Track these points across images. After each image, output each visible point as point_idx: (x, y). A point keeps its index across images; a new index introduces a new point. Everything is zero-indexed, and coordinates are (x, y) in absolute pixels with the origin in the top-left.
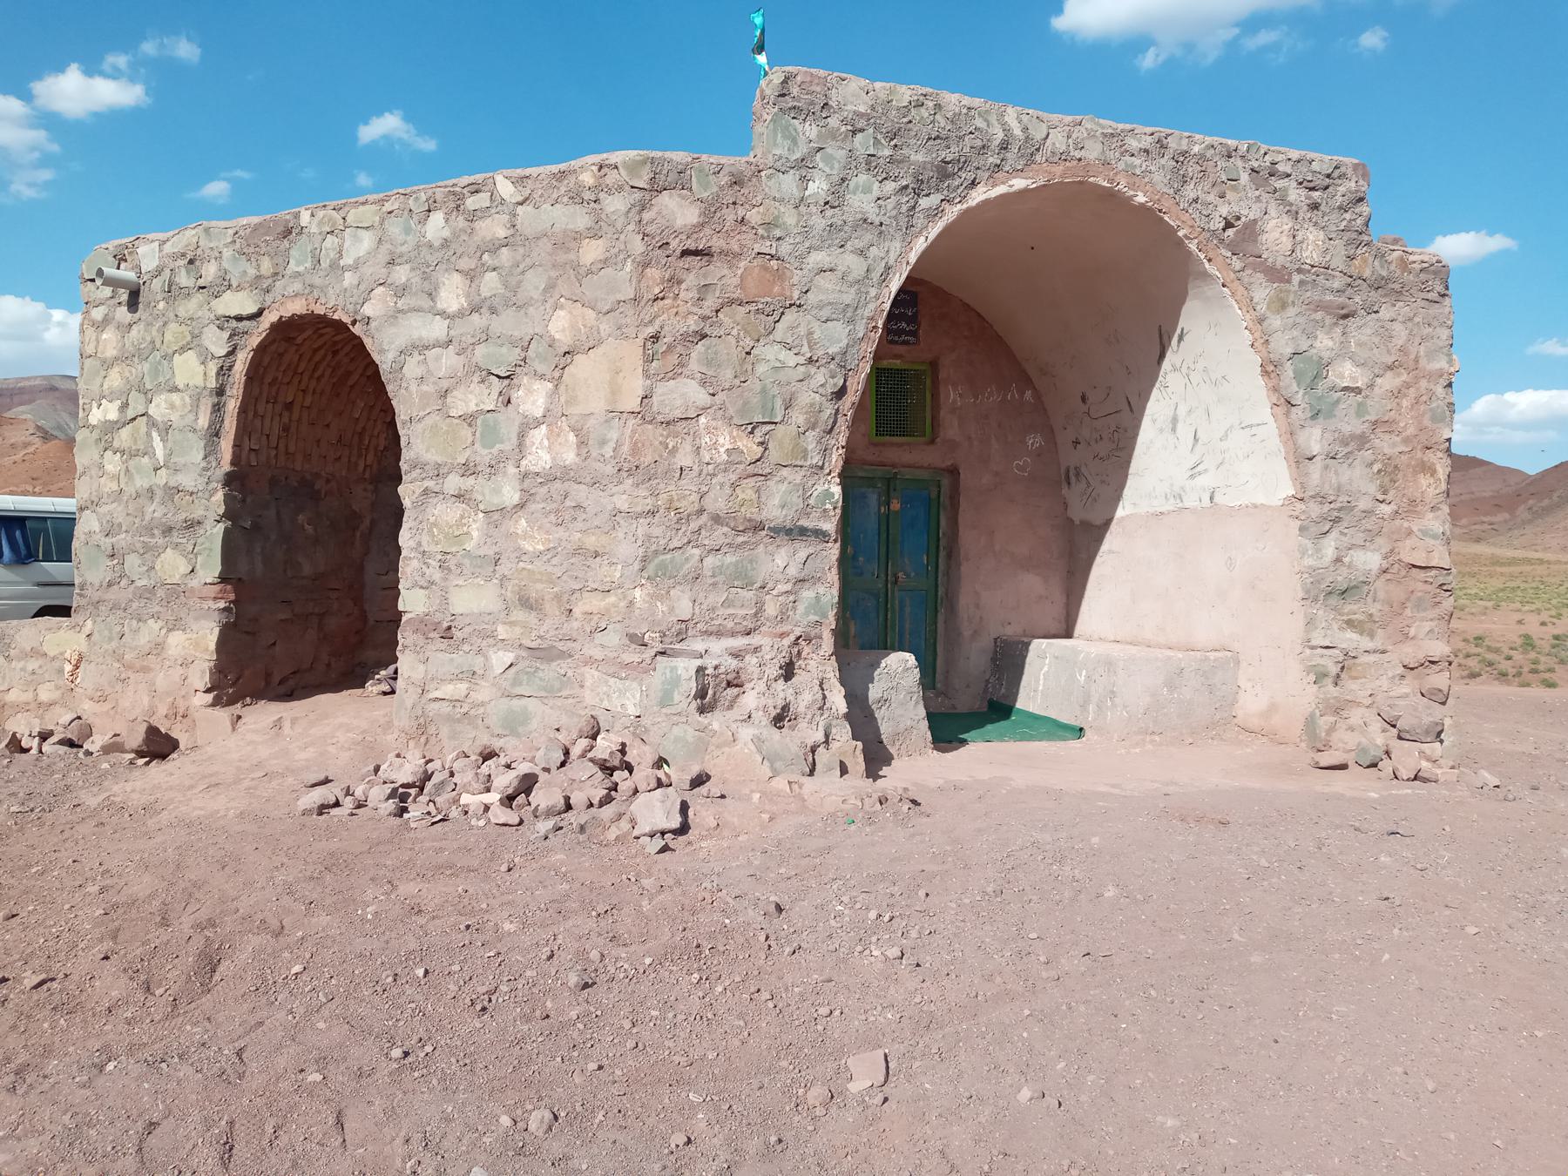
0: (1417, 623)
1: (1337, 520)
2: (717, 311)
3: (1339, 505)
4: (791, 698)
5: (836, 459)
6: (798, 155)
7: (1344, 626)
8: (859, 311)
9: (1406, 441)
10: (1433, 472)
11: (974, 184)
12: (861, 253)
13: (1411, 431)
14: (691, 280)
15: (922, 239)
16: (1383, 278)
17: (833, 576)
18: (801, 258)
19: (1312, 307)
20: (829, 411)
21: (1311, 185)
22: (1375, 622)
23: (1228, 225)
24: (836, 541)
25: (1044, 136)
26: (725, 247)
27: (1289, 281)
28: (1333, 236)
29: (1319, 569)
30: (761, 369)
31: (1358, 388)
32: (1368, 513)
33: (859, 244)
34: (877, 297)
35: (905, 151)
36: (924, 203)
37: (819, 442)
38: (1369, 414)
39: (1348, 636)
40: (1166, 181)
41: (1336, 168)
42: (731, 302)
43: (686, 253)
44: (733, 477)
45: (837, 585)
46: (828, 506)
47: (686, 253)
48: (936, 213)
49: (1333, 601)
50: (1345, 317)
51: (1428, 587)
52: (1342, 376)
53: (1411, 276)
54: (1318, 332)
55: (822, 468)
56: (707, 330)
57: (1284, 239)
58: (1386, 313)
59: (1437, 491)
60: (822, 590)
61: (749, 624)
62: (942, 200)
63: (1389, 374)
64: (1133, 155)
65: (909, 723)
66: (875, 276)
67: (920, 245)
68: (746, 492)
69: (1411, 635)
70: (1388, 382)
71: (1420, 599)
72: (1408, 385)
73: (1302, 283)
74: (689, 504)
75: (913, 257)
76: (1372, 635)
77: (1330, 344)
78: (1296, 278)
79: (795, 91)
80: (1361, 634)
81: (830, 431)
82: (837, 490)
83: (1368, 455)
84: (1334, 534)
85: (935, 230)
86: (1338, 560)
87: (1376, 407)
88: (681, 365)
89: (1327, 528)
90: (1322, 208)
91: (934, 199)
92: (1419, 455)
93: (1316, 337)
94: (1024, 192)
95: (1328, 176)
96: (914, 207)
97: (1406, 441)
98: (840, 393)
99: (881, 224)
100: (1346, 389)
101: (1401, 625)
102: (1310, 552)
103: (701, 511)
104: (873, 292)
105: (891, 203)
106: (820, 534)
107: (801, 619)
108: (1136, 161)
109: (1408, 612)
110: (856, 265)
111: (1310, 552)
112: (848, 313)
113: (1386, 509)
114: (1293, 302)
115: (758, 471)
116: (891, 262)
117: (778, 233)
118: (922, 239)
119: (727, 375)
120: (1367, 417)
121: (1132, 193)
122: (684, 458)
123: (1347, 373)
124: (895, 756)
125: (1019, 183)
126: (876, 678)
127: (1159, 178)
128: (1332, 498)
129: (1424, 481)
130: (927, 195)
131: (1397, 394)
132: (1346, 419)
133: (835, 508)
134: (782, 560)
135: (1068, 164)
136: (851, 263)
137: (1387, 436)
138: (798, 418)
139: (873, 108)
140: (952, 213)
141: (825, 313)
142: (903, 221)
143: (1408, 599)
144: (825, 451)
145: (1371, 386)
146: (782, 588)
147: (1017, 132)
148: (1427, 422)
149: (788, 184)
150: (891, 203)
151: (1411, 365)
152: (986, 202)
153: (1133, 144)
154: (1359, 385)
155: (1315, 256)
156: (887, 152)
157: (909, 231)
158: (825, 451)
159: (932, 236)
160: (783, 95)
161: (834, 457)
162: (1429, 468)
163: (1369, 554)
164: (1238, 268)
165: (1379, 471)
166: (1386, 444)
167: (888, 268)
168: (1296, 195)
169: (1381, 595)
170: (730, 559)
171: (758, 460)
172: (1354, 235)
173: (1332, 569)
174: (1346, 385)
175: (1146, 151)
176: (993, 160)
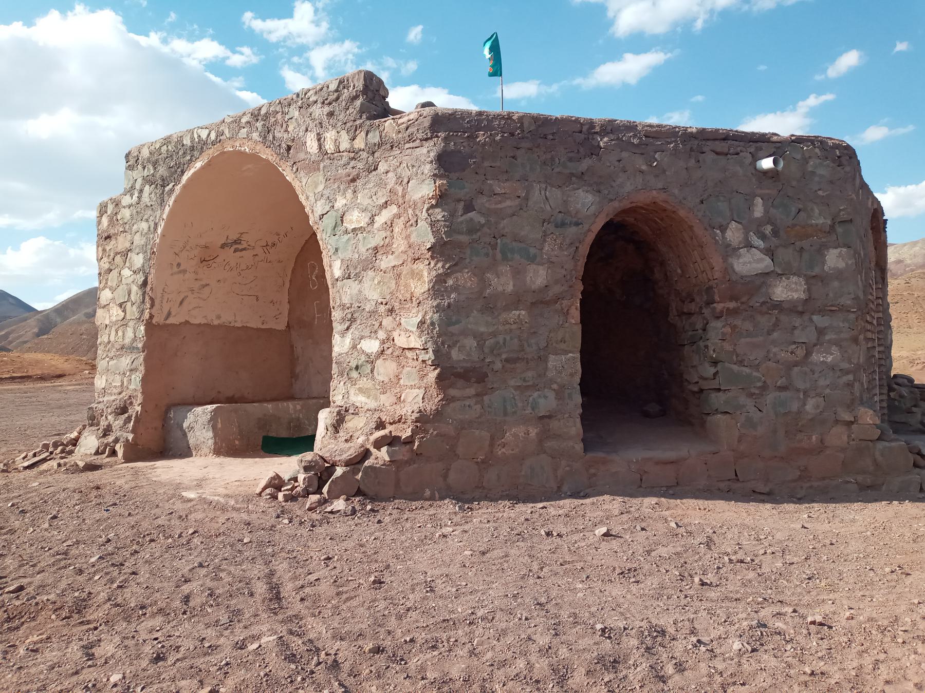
0: (407, 390)
1: (352, 320)
2: (114, 259)
3: (352, 309)
4: (111, 423)
5: (146, 315)
6: (130, 186)
7: (357, 392)
8: (148, 246)
9: (398, 257)
10: (420, 277)
11: (183, 172)
12: (147, 220)
13: (402, 248)
14: (108, 248)
15: (167, 206)
16: (375, 144)
17: (142, 368)
18: (131, 229)
19: (332, 181)
20: (140, 293)
21: (328, 101)
22: (377, 389)
23: (289, 148)
24: (143, 351)
25: (206, 136)
26: (114, 232)
27: (319, 169)
28: (339, 129)
29: (342, 353)
30: (123, 279)
31: (361, 227)
32: (373, 313)
33: (146, 217)
34: (153, 238)
35: (159, 168)
36: (167, 189)
37: (139, 307)
38: (371, 244)
39: (359, 399)
40: (258, 134)
41: (341, 82)
42: (117, 253)
43: (106, 238)
44: (117, 327)
45: (143, 372)
46: (141, 336)
47: (106, 238)
48: (172, 190)
49: (354, 374)
50: (354, 180)
51: (415, 363)
52: (351, 221)
53: (400, 135)
54: (337, 196)
55: (140, 319)
56: (111, 267)
57: (313, 142)
58: (382, 167)
59: (423, 291)
60: (138, 373)
61: (119, 390)
62: (173, 186)
63: (384, 212)
64: (244, 128)
65: (202, 439)
66: (152, 229)
67: (167, 209)
68: (120, 333)
69: (402, 398)
70: (384, 216)
71: (408, 373)
72: (399, 216)
73: (324, 167)
74: (106, 340)
75: (165, 216)
76: (376, 399)
77: (344, 201)
78: (322, 165)
79: (130, 158)
80: (368, 397)
81: (143, 302)
82: (142, 328)
83: (371, 273)
84: (351, 331)
85: (171, 202)
86: (354, 347)
87: (376, 240)
88: (107, 283)
89: (346, 327)
90: (335, 113)
91: (171, 186)
92: (409, 264)
93: (336, 201)
94: (202, 168)
95: (337, 91)
96: (163, 193)
97: (398, 257)
98: (145, 283)
99: (152, 205)
100: (354, 230)
101: (395, 391)
102: (338, 343)
103: (109, 342)
104: (151, 236)
105: (153, 195)
106: (137, 348)
107: (132, 387)
108: (245, 130)
109: (402, 382)
110: (144, 226)
111: (338, 343)
112: (143, 248)
113: (382, 309)
114: (321, 181)
115: (123, 323)
116: (157, 221)
117: (126, 221)
118: (167, 206)
119: (114, 285)
120: (369, 246)
121: (243, 149)
122: (107, 322)
123: (355, 219)
124: (194, 455)
125: (198, 165)
126: (188, 416)
127: (255, 136)
128: (348, 305)
129: (413, 284)
130: (168, 185)
131: (390, 225)
132: (356, 250)
133: (143, 337)
134: (125, 362)
135: (215, 146)
136: (144, 226)
137: (384, 257)
138: (133, 298)
139: (150, 153)
140: (178, 188)
141: (137, 251)
142: (159, 201)
143: (401, 372)
144: (142, 312)
145: (372, 222)
146: (128, 374)
147: (197, 140)
148: (413, 238)
149: (126, 200)
150: (153, 195)
151: (401, 201)
152: (190, 180)
153: (244, 120)
154: (362, 225)
155: (331, 147)
156: (152, 172)
157: (162, 203)
158: (142, 312)
159: (171, 204)
160: (127, 162)
161: (146, 313)
162: (417, 273)
163: (373, 341)
164: (294, 171)
165: (379, 283)
166: (386, 262)
167: (156, 225)
168: (319, 111)
169: (382, 370)
170: (115, 361)
171: (124, 319)
172: (351, 123)
173: (350, 353)
174: (353, 227)
175: (248, 122)
176: (188, 158)
